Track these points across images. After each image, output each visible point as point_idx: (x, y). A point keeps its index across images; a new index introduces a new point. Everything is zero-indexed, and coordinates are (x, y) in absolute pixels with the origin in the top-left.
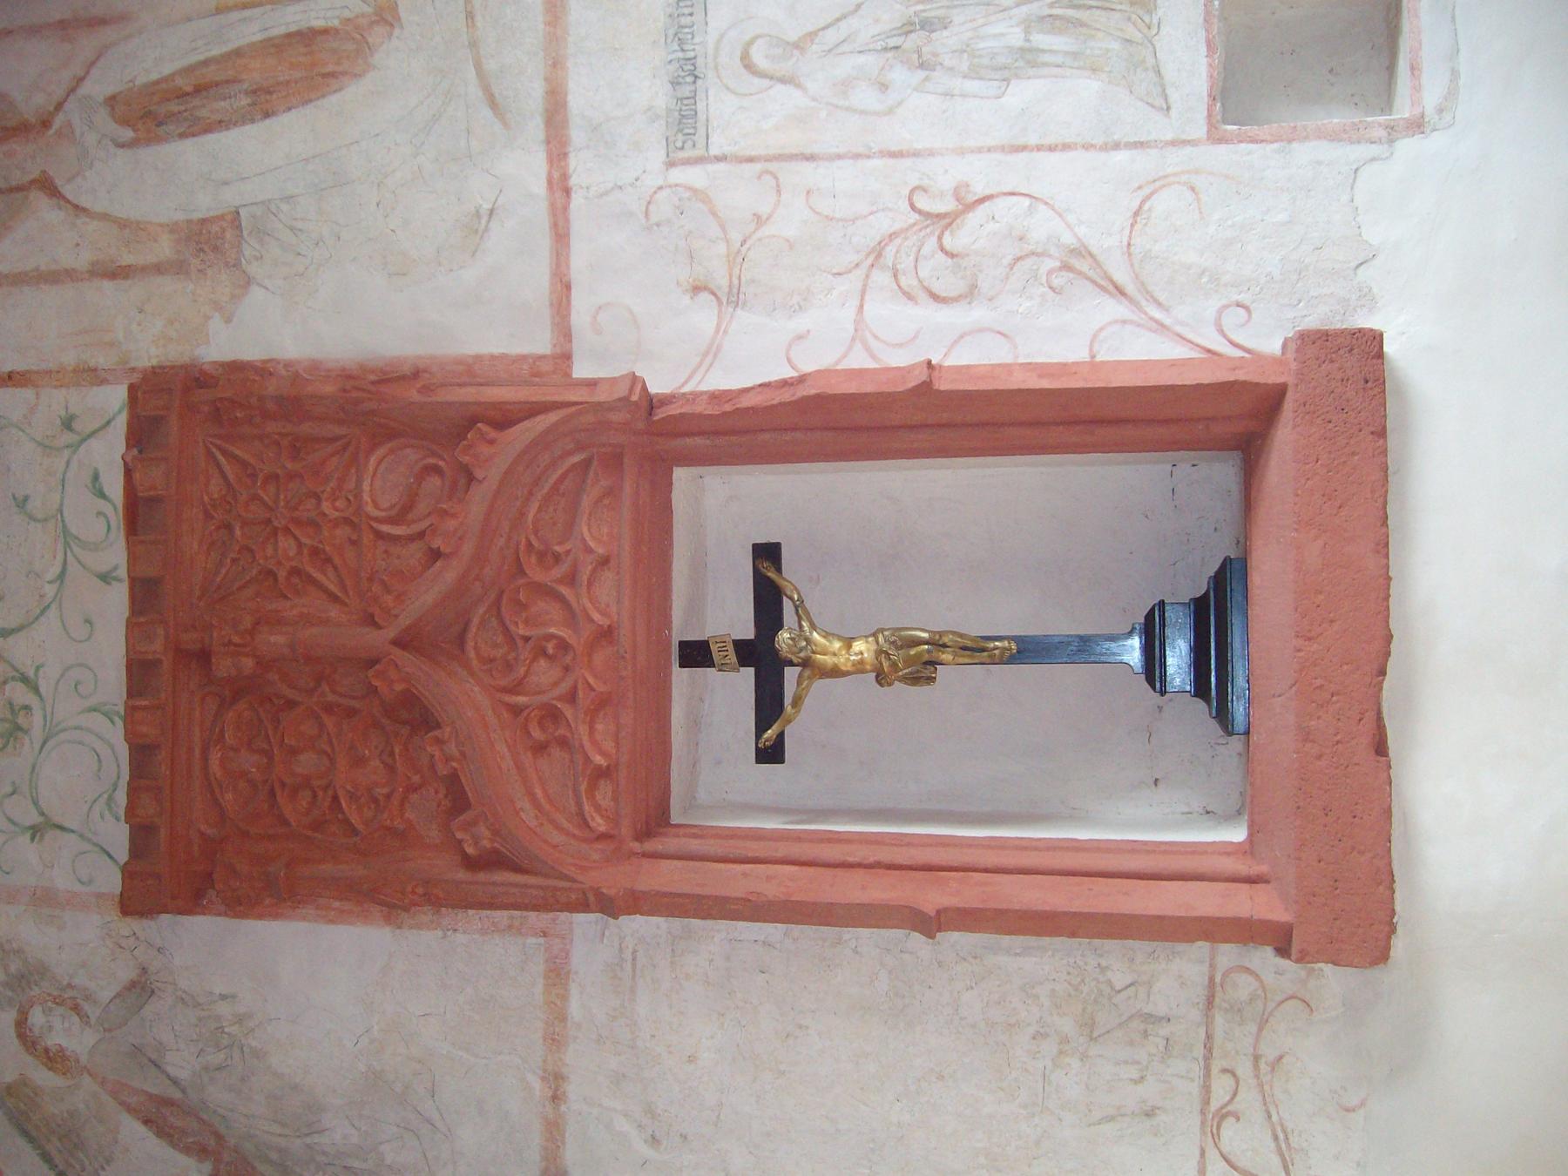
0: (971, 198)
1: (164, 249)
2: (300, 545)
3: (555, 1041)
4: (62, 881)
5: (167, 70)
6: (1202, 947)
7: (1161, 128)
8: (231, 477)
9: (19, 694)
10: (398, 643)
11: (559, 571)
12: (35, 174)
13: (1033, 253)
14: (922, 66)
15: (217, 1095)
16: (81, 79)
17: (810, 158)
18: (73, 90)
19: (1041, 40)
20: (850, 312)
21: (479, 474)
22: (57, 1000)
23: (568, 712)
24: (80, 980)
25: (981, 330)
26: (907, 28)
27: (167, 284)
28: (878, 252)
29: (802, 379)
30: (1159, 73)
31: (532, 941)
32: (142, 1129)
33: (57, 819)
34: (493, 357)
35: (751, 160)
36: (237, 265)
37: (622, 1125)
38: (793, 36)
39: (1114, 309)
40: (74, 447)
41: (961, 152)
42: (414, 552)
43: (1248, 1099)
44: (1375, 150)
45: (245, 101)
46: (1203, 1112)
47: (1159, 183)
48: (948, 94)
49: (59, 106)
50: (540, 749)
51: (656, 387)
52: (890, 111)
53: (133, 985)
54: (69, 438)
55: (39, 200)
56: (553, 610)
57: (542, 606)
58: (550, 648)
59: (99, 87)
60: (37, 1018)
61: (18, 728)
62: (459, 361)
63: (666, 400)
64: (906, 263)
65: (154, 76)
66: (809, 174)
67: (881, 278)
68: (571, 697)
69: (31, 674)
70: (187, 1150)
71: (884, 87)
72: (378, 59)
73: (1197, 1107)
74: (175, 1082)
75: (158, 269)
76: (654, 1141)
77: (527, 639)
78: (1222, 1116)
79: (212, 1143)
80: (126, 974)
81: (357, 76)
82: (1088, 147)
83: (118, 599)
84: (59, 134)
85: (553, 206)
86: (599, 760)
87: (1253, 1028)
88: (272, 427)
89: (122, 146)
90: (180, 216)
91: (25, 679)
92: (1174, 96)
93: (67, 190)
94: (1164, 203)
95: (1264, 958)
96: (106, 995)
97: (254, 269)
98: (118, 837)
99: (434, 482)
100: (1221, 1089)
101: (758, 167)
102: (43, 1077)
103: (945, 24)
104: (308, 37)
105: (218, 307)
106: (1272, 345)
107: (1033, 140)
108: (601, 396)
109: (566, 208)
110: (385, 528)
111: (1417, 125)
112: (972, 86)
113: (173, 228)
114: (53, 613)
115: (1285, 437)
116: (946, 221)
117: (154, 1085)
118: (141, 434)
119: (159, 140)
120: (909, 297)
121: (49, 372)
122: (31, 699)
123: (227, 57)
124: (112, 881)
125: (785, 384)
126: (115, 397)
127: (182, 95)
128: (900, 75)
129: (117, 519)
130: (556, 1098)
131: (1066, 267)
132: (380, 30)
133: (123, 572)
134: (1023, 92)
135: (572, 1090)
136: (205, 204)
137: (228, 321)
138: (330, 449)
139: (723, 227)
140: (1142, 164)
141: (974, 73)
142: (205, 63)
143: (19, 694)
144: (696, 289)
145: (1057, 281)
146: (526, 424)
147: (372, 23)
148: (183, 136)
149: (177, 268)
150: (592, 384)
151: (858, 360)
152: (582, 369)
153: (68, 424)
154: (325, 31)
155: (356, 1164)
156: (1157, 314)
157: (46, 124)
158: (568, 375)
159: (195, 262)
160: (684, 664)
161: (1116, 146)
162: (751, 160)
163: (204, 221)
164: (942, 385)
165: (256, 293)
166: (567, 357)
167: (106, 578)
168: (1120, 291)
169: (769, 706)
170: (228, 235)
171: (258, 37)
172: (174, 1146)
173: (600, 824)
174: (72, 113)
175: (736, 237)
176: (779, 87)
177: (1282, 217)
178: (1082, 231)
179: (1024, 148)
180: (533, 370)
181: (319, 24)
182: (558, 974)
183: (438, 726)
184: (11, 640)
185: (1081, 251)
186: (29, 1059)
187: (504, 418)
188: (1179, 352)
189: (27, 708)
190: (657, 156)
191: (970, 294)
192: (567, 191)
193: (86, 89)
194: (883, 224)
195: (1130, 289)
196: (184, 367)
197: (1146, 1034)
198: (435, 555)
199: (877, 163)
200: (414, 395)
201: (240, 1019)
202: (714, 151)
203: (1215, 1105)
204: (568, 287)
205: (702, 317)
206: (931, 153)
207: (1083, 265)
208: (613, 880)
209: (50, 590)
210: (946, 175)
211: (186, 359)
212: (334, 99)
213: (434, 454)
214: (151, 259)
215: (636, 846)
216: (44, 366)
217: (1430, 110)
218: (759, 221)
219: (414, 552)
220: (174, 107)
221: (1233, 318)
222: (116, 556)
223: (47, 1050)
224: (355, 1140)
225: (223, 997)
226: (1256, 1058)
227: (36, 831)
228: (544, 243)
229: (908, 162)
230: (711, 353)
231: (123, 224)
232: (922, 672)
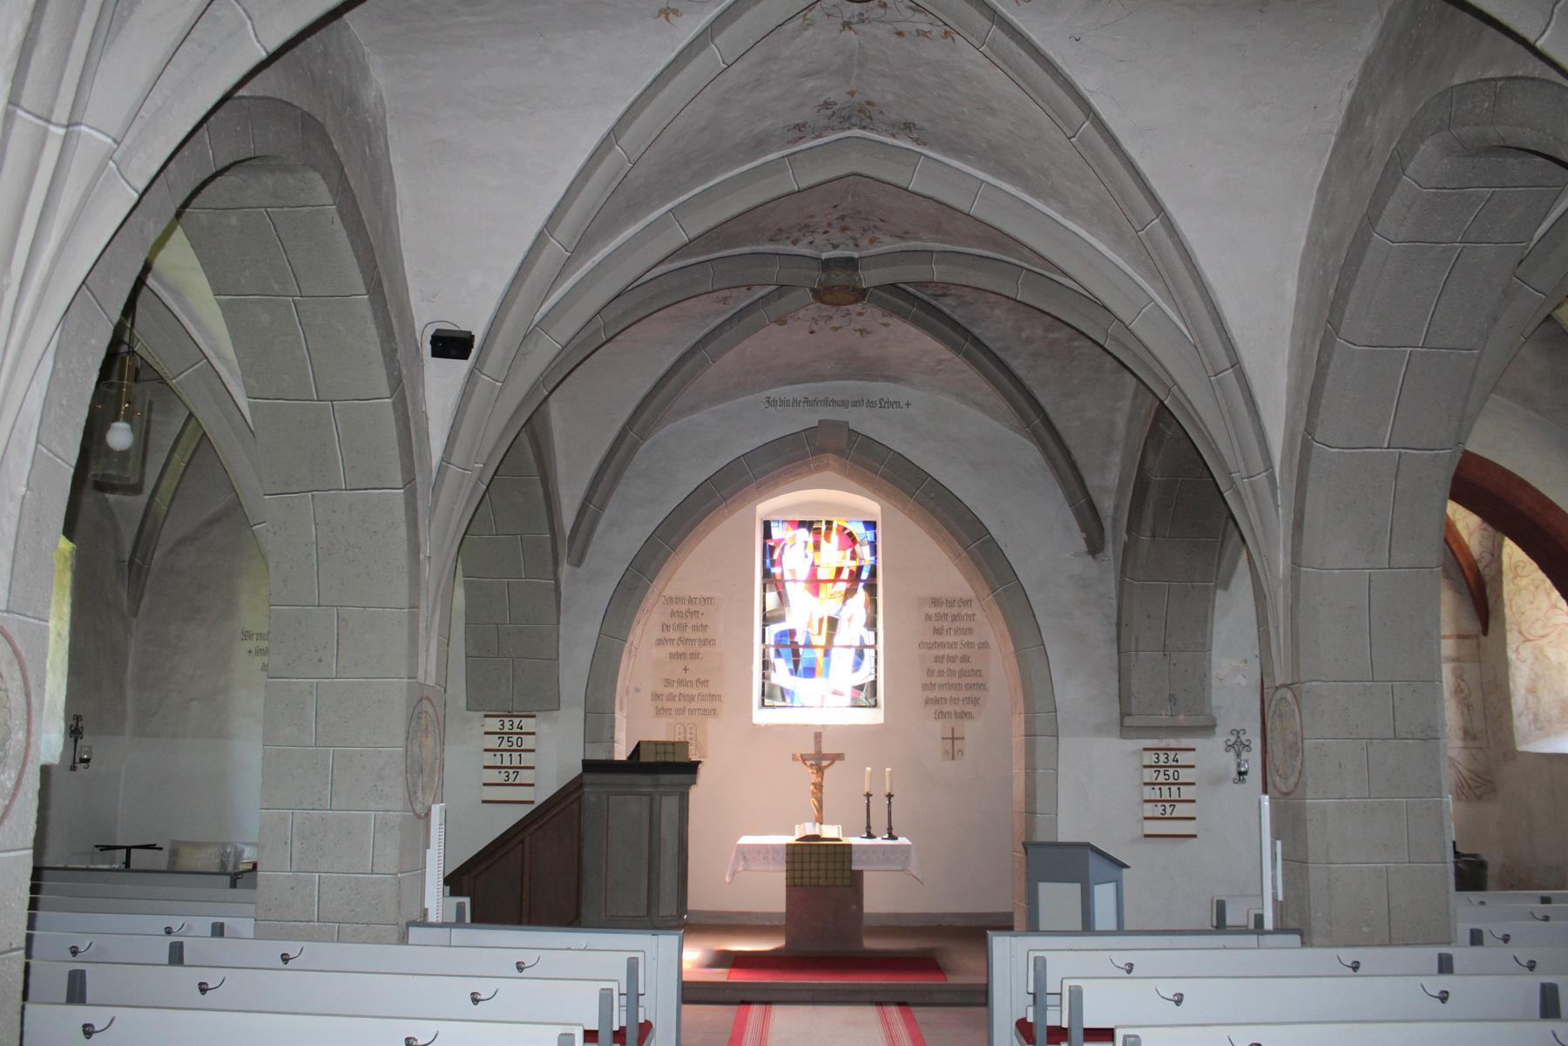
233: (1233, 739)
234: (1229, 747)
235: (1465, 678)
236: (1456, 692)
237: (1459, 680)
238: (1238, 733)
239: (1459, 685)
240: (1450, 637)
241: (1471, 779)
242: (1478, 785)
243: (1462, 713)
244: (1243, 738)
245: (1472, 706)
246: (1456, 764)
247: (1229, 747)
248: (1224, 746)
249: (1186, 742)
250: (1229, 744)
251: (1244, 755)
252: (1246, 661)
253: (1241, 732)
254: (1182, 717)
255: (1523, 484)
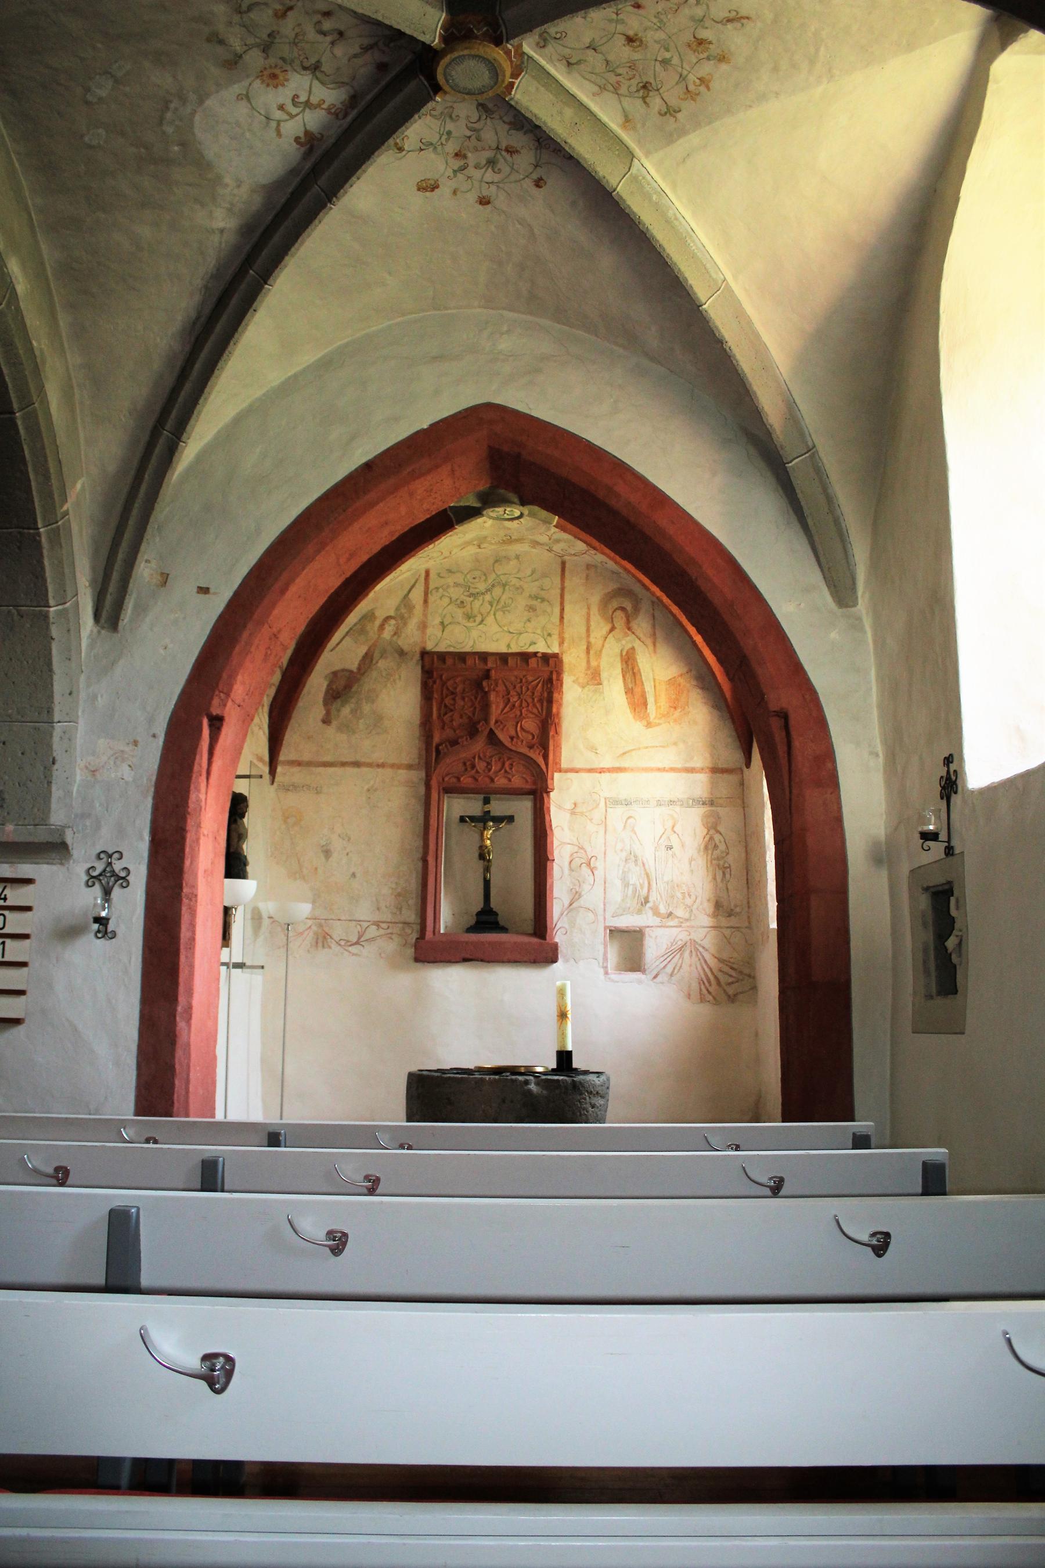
0: (594, 870)
1: (594, 663)
2: (516, 702)
3: (393, 766)
4: (429, 631)
5: (640, 665)
6: (419, 921)
7: (608, 915)
8: (533, 683)
9: (479, 619)
10: (491, 729)
11: (508, 769)
12: (616, 625)
13: (580, 885)
14: (626, 860)
15: (374, 674)
16: (640, 639)
17: (605, 832)
18: (637, 637)
19: (631, 888)
20: (569, 841)
21: (531, 751)
22: (397, 628)
23: (474, 771)
24: (403, 635)
25: (563, 873)
26: (635, 856)
27: (584, 664)
28: (582, 848)
29: (552, 830)
30: (621, 915)
31: (417, 761)
32: (364, 651)
33: (446, 629)
34: (561, 752)
35: (606, 818)
36: (588, 684)
37: (372, 782)
38: (635, 829)
39: (567, 903)
40: (543, 637)
41: (605, 869)
42: (513, 733)
43: (382, 932)
44: (601, 964)
45: (630, 687)
46: (379, 921)
47: (596, 915)
48: (619, 866)
49: (633, 633)
50: (465, 764)
51: (552, 794)
52: (616, 852)
53: (402, 650)
54: (546, 634)
55: (608, 627)
56: (498, 768)
57: (499, 765)
58: (489, 767)
59: (637, 644)
60: (393, 622)
61: (470, 618)
62: (560, 744)
63: (549, 796)
64: (579, 855)
65: (638, 661)
66: (602, 832)
67: (576, 849)
68: (477, 772)
69: (484, 623)
70: (359, 665)
71: (622, 850)
72: (638, 723)
73: (381, 920)
74: (377, 662)
75: (588, 662)
76: (368, 790)
77: (491, 761)
78: (378, 926)
79: (362, 671)
80: (406, 648)
81: (634, 717)
82: (605, 898)
83: (503, 649)
84: (627, 633)
85: (597, 769)
86: (462, 779)
87: (399, 933)
88: (545, 695)
89: (621, 651)
90: (602, 668)
91: (482, 621)
92: (616, 918)
93: (611, 635)
94: (590, 914)
95: (415, 936)
96: (400, 643)
97: (586, 689)
98: (442, 648)
99: (530, 737)
100: (384, 925)
101: (604, 819)
102: (378, 623)
103: (636, 865)
104: (645, 704)
105: (577, 679)
106: (557, 940)
107: (607, 885)
108: (549, 782)
109: (596, 772)
110: (519, 725)
111: (606, 973)
112: (621, 872)
113: (599, 666)
114: (501, 630)
115: (535, 940)
116: (589, 864)
117: (377, 655)
118: (546, 658)
119: (622, 661)
120: (572, 855)
121: (563, 629)
122: (477, 622)
123: (642, 682)
124: (430, 646)
125: (551, 826)
126: (555, 649)
127: (633, 669)
128: (624, 854)
129: (524, 649)
130: (378, 766)
131: (577, 892)
132: (645, 723)
133: (510, 651)
134: (618, 883)
135: (380, 770)
136: (604, 675)
137: (574, 682)
138: (540, 710)
139: (590, 811)
140: (600, 911)
141: (624, 872)
142: (641, 675)
143: (479, 619)
144: (575, 804)
145: (574, 891)
146: (543, 762)
147: (647, 721)
148: (622, 669)
149: (589, 667)
150: (552, 779)
151: (555, 843)
152: (556, 775)
153: (549, 635)
154: (646, 708)
155: (358, 712)
156: (565, 913)
157: (629, 629)
158: (556, 772)
159: (589, 672)
160: (484, 797)
161: (604, 905)
162: (606, 818)
163: (600, 674)
164: (549, 863)
165: (580, 690)
166: (560, 771)
167: (509, 646)
168: (571, 905)
169: (473, 819)
170: (596, 682)
171: (646, 690)
172: (361, 661)
173: (446, 779)
174: (632, 637)
175: (587, 814)
176: (623, 825)
177: (586, 942)
178: (585, 896)
179: (605, 883)
180: (557, 763)
181: (648, 707)
182: (410, 767)
183: (471, 739)
184: (493, 617)
185: (580, 896)
186: (381, 620)
187: (546, 757)
188: (555, 919)
189: (475, 621)
190: (608, 795)
191: (571, 869)
192: (600, 773)
193: (637, 641)
194: (588, 849)
195: (571, 907)
196: (562, 670)
197: (397, 908)
198: (512, 738)
199: (603, 848)
200: (551, 734)
201: (394, 681)
202: (608, 809)
203: (381, 924)
204: (577, 772)
205: (569, 806)
206: (605, 861)
207: (577, 896)
208: (434, 783)
209: (506, 629)
210: (599, 864)
211: (564, 669)
212: (628, 711)
213: (537, 737)
214: (591, 660)
215: (441, 788)
216: (565, 627)
217: (609, 976)
218: (591, 820)
219: (513, 733)
220: (630, 667)
221: (563, 931)
222: (514, 649)
223: (384, 625)
224: (365, 712)
225: (400, 676)
226: (392, 934)
227: (442, 623)
228: (588, 767)
229: (603, 856)
230: (560, 807)
231: (601, 651)
232: (482, 857)
233: (100, 867)
234: (92, 879)
235: (720, 828)
236: (706, 848)
237: (712, 832)
238: (110, 856)
239: (711, 838)
240: (701, 770)
241: (721, 971)
242: (731, 980)
243: (715, 878)
244: (117, 866)
245: (729, 867)
246: (701, 949)
247: (92, 879)
248: (85, 878)
249: (25, 870)
250: (95, 874)
251: (117, 892)
252: (136, 743)
253: (116, 856)
254: (10, 827)
255: (620, 468)
